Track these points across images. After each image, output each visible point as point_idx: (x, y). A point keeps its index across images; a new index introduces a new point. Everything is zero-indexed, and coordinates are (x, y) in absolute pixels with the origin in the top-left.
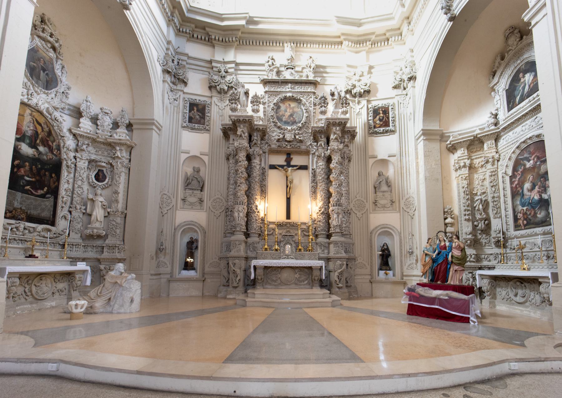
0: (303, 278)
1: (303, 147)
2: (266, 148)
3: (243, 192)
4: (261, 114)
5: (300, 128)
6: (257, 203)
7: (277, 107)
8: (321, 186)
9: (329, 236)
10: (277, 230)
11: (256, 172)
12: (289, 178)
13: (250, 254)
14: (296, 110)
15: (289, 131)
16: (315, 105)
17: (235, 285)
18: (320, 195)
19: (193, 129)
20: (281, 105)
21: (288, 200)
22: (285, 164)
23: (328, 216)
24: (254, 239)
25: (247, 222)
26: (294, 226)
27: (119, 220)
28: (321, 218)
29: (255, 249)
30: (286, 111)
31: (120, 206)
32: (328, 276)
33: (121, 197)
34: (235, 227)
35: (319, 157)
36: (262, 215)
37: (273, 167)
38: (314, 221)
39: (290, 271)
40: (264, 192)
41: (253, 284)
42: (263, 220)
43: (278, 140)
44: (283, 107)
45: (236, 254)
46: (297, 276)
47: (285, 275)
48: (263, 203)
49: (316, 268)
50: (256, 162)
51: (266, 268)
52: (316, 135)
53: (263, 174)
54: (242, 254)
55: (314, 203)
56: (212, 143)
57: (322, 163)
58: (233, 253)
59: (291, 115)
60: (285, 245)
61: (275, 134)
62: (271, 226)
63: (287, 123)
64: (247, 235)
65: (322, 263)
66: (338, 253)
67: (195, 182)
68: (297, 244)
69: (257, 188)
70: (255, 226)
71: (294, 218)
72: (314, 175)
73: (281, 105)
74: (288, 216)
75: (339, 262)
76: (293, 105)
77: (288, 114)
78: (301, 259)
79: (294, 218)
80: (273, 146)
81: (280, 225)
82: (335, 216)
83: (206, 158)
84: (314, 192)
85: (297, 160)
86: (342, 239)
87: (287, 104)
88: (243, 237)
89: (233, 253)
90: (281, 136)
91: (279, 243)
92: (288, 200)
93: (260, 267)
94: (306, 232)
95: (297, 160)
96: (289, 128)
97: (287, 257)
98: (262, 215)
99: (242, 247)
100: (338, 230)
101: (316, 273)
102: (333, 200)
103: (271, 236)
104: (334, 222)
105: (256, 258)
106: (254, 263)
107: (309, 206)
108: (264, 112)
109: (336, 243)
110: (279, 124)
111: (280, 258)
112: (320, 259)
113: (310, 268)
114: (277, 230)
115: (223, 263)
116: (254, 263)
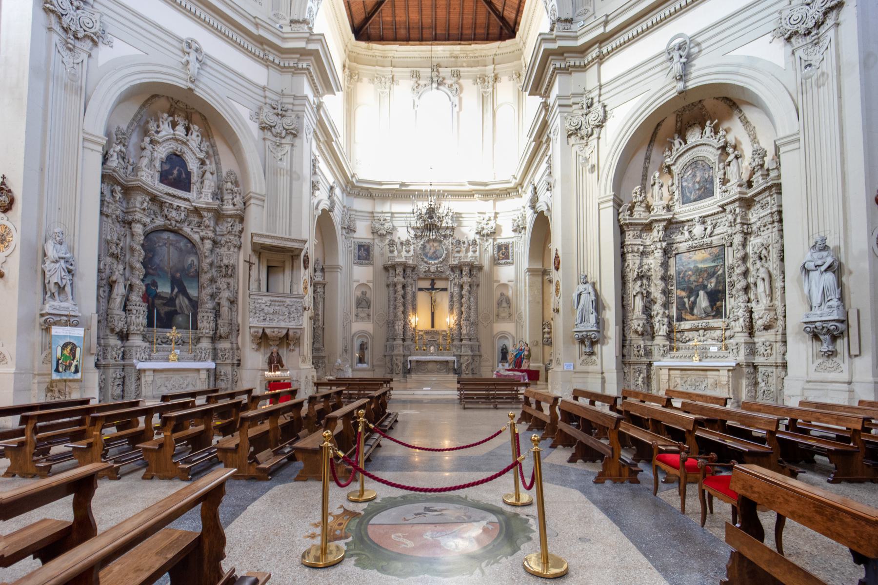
0: (442, 368)
1: (444, 276)
2: (415, 277)
3: (401, 312)
4: (412, 253)
5: (441, 262)
6: (410, 318)
7: (424, 247)
8: (456, 305)
9: (461, 340)
10: (425, 336)
11: (409, 297)
12: (433, 298)
13: (406, 353)
14: (438, 248)
15: (433, 265)
16: (452, 244)
17: (398, 372)
18: (455, 311)
19: (361, 264)
20: (427, 245)
21: (433, 314)
22: (430, 287)
23: (460, 328)
24: (408, 342)
25: (403, 332)
26: (437, 333)
27: (320, 332)
28: (456, 327)
29: (409, 349)
30: (430, 249)
31: (321, 323)
32: (460, 367)
33: (320, 318)
34: (396, 336)
35: (455, 284)
36: (413, 325)
37: (421, 290)
38: (451, 329)
39: (434, 364)
40: (414, 309)
41: (409, 371)
42: (414, 329)
43: (425, 272)
44: (428, 246)
45: (398, 353)
46: (438, 366)
47: (430, 366)
48: (414, 317)
49: (451, 362)
50: (409, 289)
51: (417, 362)
52: (453, 269)
53: (414, 296)
54: (401, 352)
55: (452, 316)
56: (375, 273)
57: (456, 289)
58: (395, 352)
59: (434, 252)
60: (430, 346)
61: (423, 267)
62: (421, 333)
63: (431, 258)
64: (404, 340)
65: (454, 358)
66: (466, 352)
67: (364, 303)
68: (439, 345)
69: (410, 307)
70: (409, 333)
71: (437, 328)
72: (452, 296)
73: (427, 245)
74: (433, 326)
75: (466, 358)
76: (435, 244)
77: (432, 251)
78: (442, 356)
79: (437, 328)
80: (421, 276)
81: (427, 333)
82: (465, 327)
83: (371, 285)
84: (451, 309)
85: (439, 284)
86: (470, 343)
87: (431, 244)
88: (401, 342)
89: (395, 352)
90: (427, 269)
91: (426, 345)
92: (433, 314)
93: (414, 361)
94: (445, 337)
95: (439, 284)
96: (433, 262)
97: (432, 354)
98: (413, 325)
99: (401, 348)
100: (466, 337)
101: (451, 365)
102: (464, 316)
103: (420, 341)
104: (464, 331)
105: (410, 355)
106: (410, 358)
107: (448, 320)
108: (414, 250)
109: (465, 345)
110: (425, 260)
111: (426, 355)
112: (454, 356)
113: (447, 362)
114: (425, 336)
115: (388, 359)
116: (410, 358)
